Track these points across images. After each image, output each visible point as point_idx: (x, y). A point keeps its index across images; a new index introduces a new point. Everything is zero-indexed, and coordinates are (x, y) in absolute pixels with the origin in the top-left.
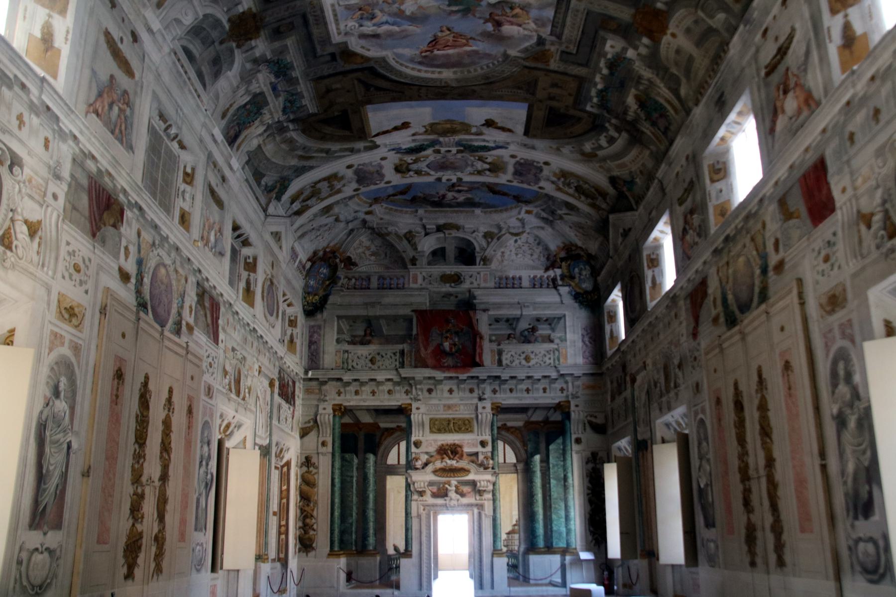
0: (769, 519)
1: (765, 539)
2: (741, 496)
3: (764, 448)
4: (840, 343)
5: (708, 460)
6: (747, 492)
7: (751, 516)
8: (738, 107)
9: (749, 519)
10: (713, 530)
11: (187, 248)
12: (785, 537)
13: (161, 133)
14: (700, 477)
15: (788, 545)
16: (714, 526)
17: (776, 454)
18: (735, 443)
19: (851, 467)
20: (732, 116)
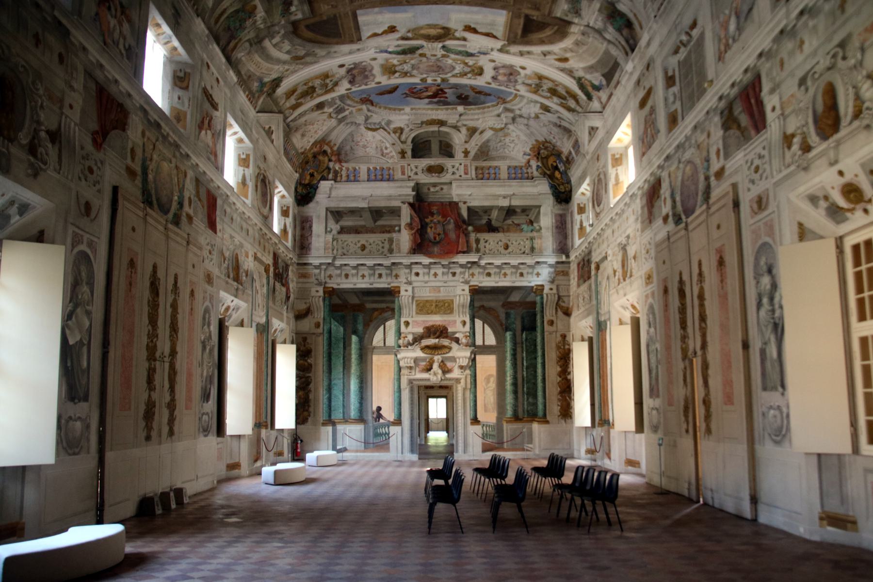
0: (167, 398)
1: (162, 416)
2: (146, 373)
3: (171, 340)
4: (207, 303)
5: (88, 313)
6: (151, 372)
7: (152, 393)
8: (181, 50)
9: (150, 396)
10: (84, 405)
11: (708, 102)
12: (176, 413)
13: (689, 48)
14: (67, 326)
15: (177, 419)
16: (86, 399)
17: (178, 349)
18: (146, 320)
19: (205, 374)
20: (176, 43)
